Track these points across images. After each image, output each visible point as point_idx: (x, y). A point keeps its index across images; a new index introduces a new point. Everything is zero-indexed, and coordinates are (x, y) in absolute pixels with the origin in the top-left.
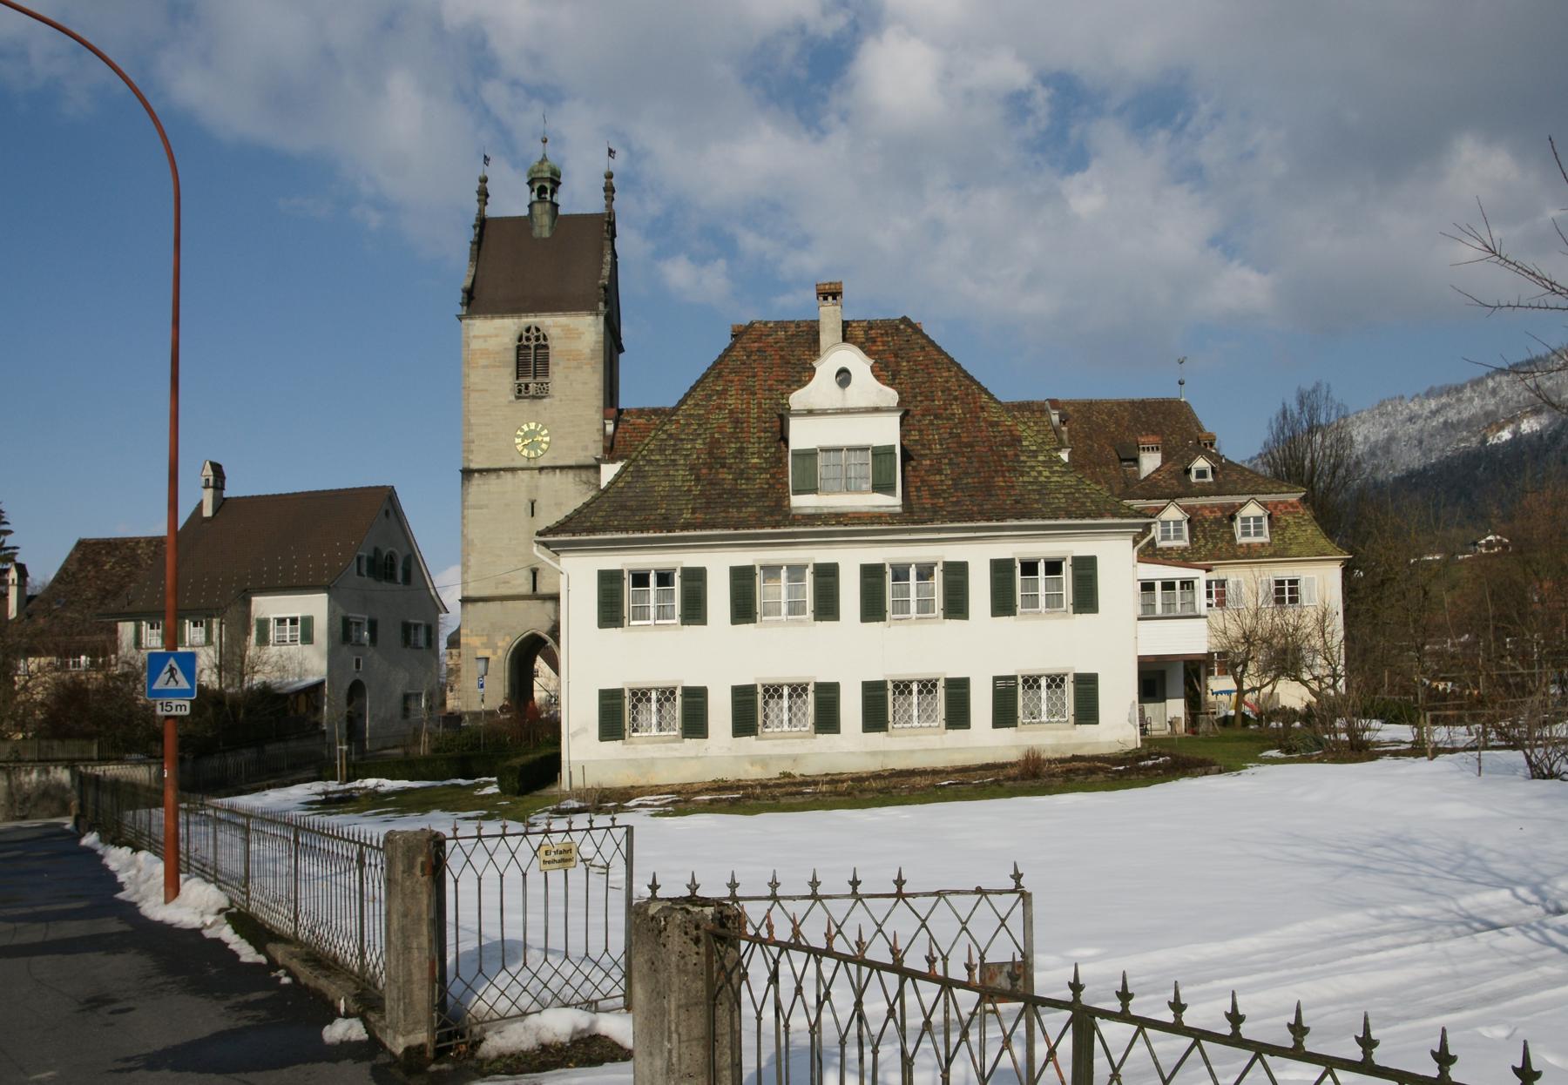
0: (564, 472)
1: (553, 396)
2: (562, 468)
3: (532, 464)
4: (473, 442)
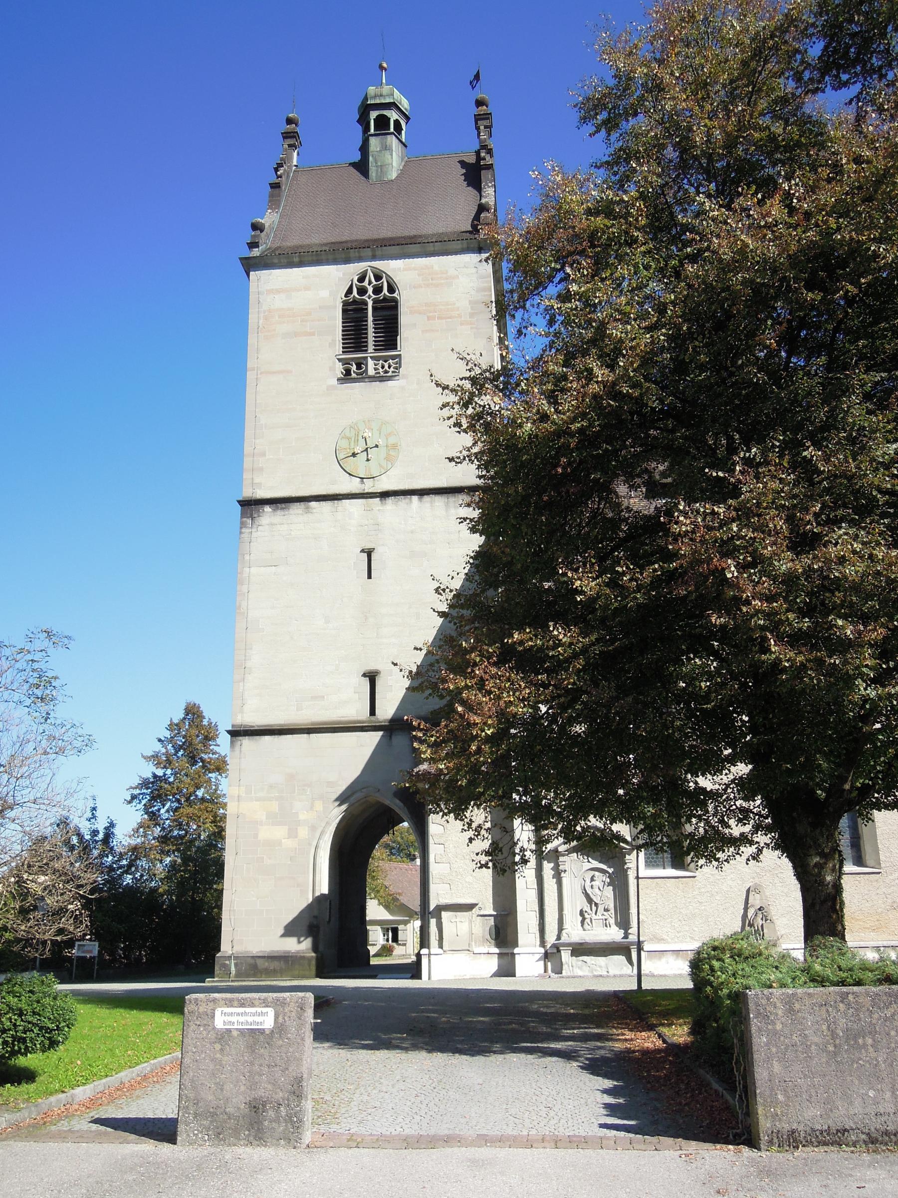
0: (426, 498)
1: (405, 377)
2: (422, 493)
3: (369, 487)
4: (263, 454)
